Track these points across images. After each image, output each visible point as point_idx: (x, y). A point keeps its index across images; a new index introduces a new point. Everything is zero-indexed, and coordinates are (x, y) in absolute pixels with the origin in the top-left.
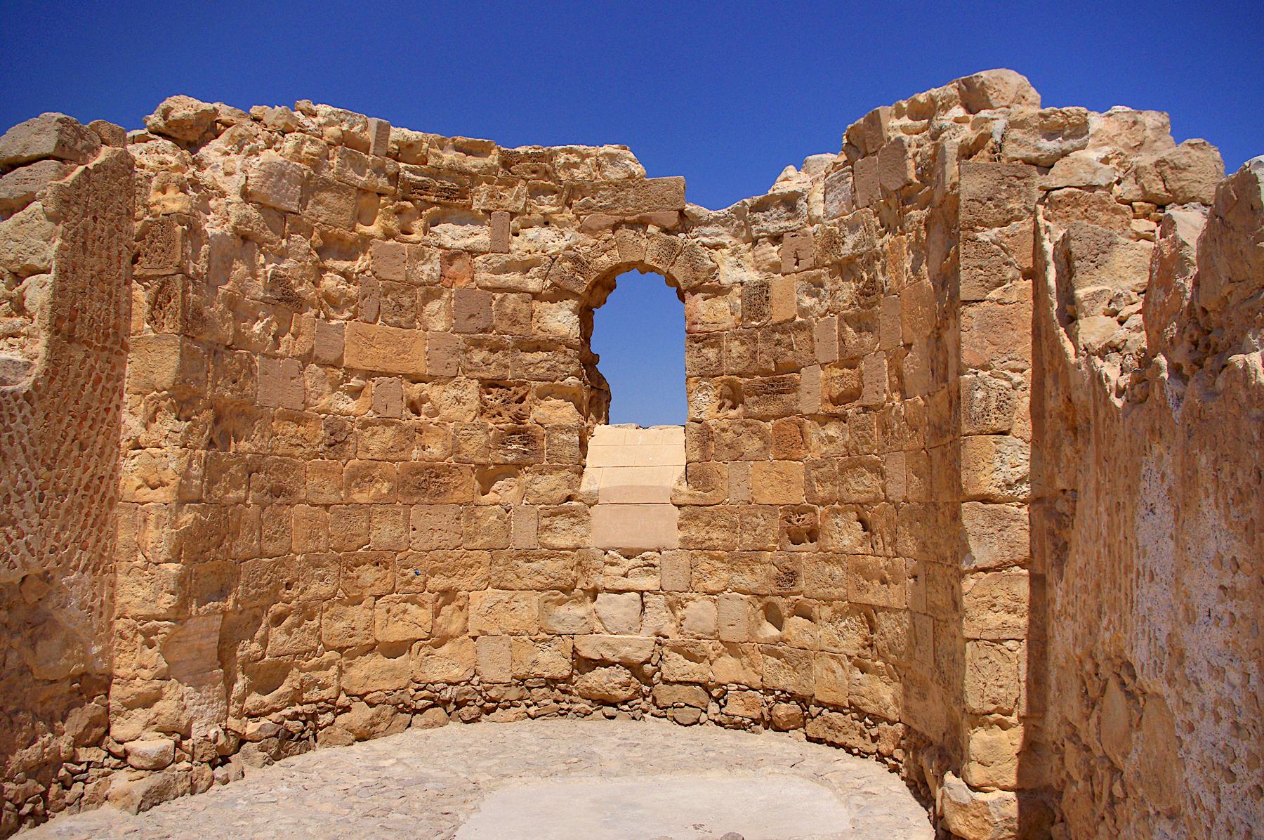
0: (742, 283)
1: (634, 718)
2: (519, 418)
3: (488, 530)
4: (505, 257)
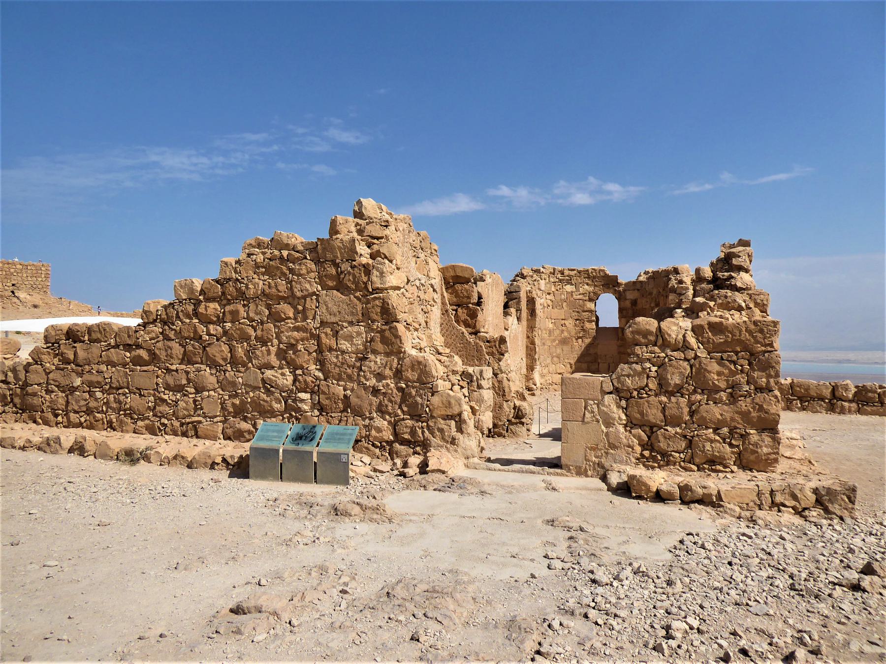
4: (579, 293)
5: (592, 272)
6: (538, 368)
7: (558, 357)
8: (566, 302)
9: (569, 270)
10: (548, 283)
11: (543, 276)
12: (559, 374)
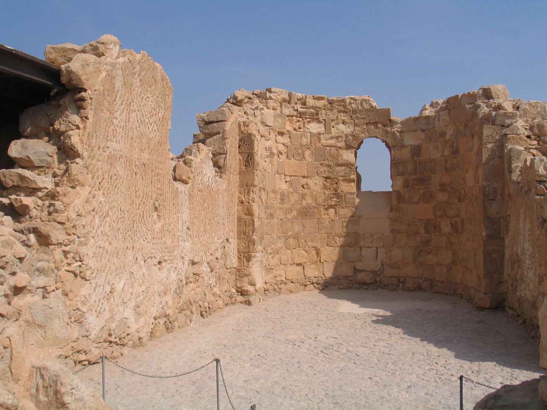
0: (411, 145)
1: (374, 289)
2: (335, 190)
3: (327, 227)
4: (330, 135)
5: (350, 103)
6: (258, 256)
7: (296, 237)
8: (309, 148)
9: (314, 98)
10: (279, 116)
11: (271, 103)
12: (298, 265)
